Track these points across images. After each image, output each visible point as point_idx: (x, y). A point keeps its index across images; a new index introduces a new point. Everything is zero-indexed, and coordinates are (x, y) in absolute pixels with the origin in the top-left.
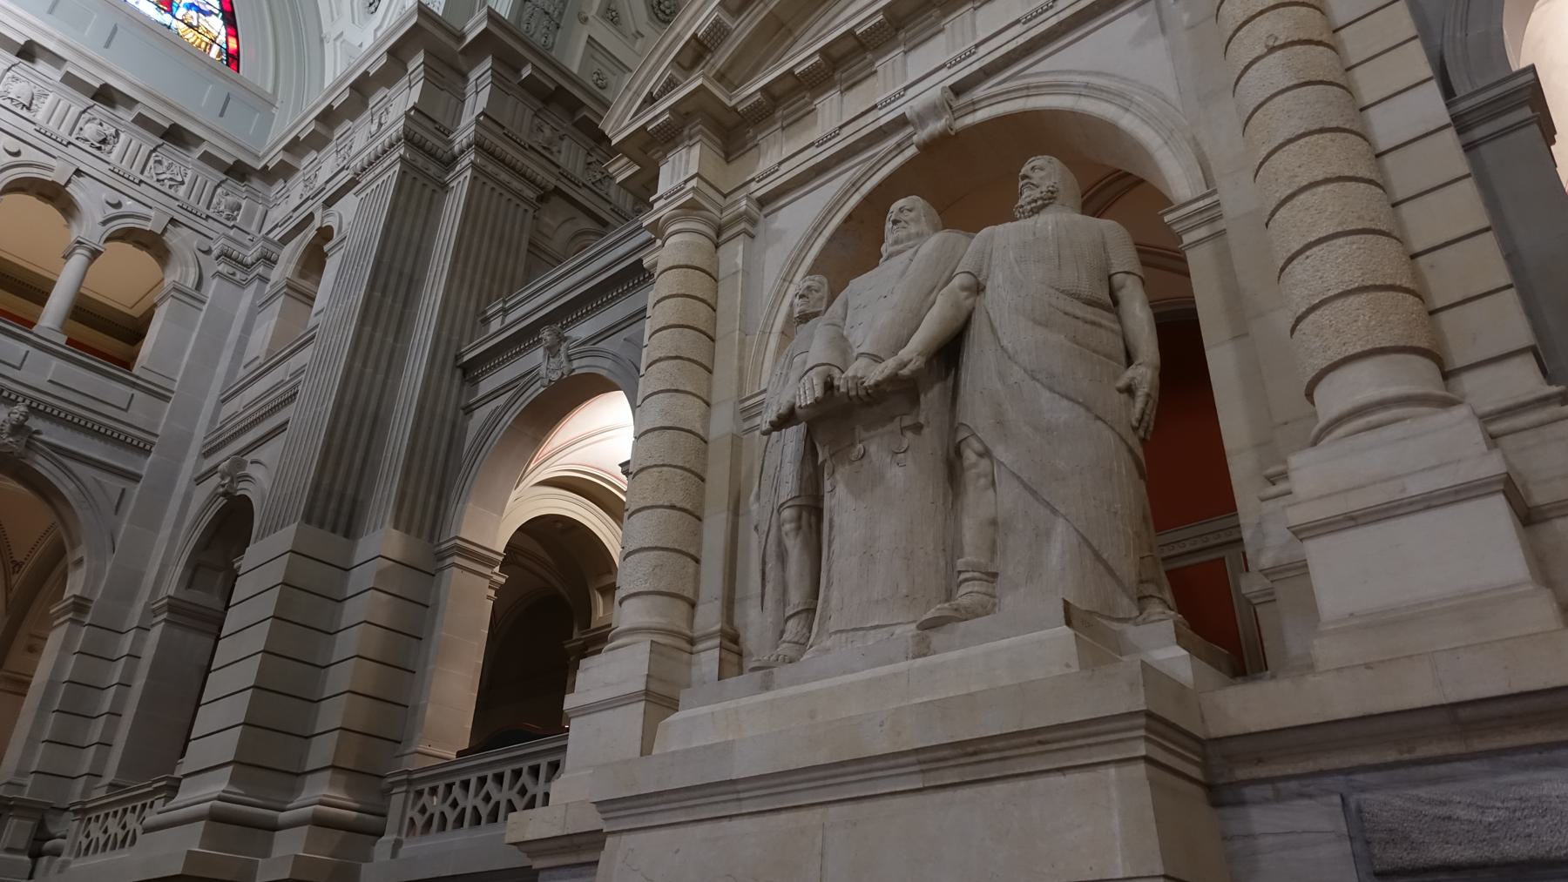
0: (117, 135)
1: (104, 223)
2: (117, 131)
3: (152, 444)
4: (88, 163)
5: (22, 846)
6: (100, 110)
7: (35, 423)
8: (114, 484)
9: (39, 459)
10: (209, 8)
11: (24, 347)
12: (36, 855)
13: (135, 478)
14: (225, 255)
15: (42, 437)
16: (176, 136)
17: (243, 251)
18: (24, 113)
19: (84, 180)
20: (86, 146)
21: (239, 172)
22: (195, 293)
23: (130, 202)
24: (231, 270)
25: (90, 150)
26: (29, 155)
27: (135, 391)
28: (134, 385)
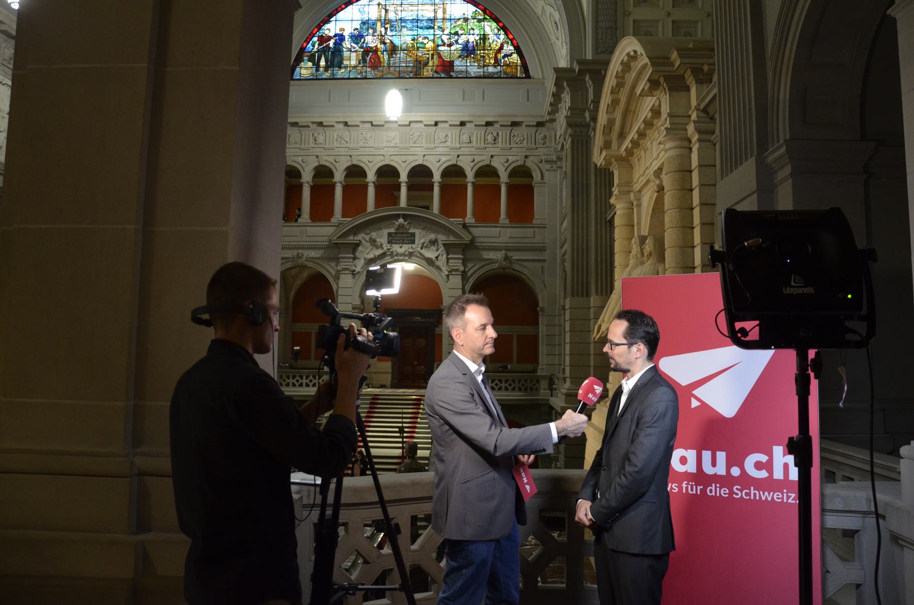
0: (498, 134)
1: (506, 171)
2: (498, 134)
3: (546, 247)
4: (493, 151)
5: (546, 388)
6: (489, 128)
7: (510, 254)
8: (538, 265)
9: (515, 265)
10: (510, 52)
11: (498, 229)
12: (551, 389)
13: (544, 261)
14: (547, 161)
15: (513, 258)
16: (515, 124)
17: (551, 157)
18: (470, 145)
19: (495, 158)
20: (490, 145)
21: (540, 124)
22: (542, 181)
23: (510, 157)
24: (550, 166)
25: (492, 146)
26: (477, 159)
27: (535, 229)
28: (533, 227)
